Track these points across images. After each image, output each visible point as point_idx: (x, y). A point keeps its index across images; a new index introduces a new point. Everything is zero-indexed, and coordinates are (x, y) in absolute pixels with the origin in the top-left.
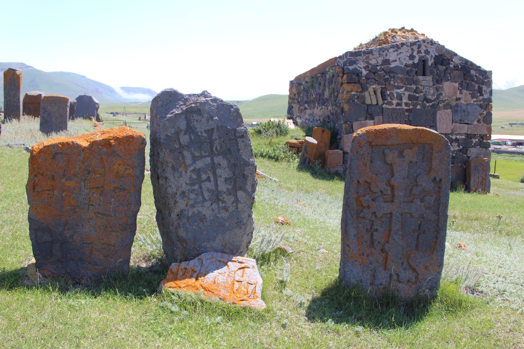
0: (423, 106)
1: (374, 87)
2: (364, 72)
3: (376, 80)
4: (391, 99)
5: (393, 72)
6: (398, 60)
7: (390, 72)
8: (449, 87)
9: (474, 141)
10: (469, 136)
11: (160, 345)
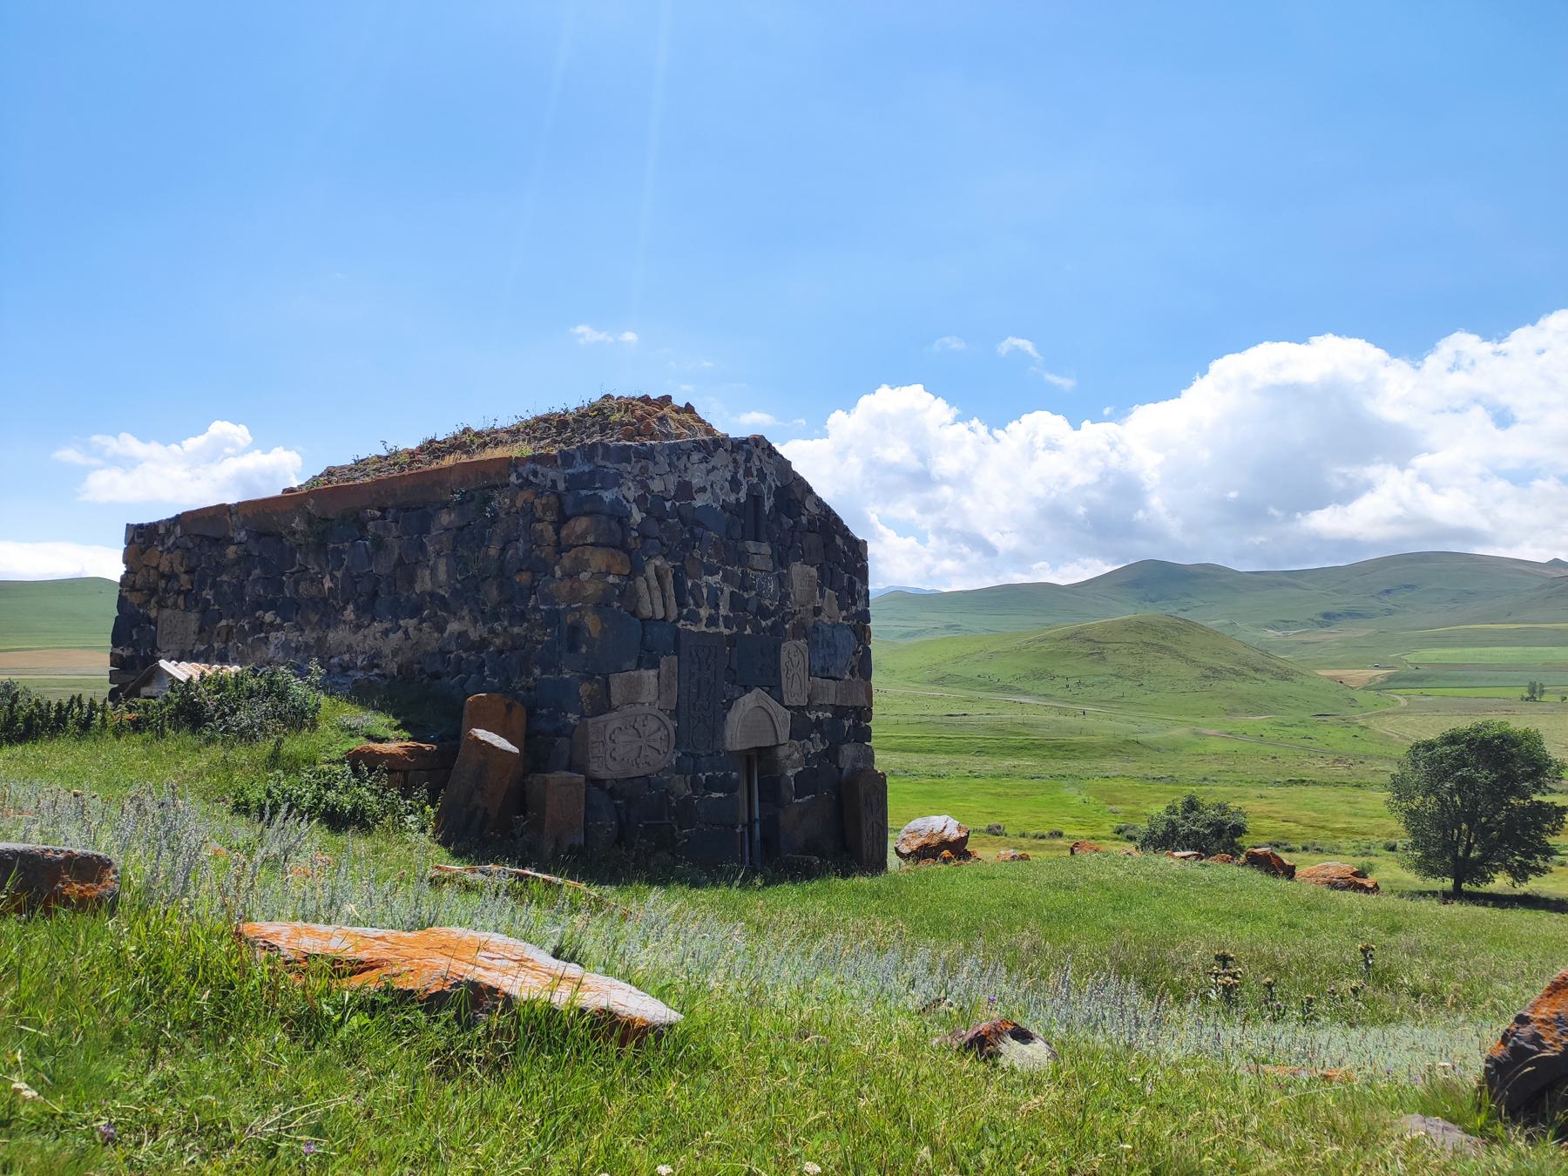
0: (757, 628)
2: (637, 516)
3: (663, 544)
5: (699, 524)
7: (693, 522)
10: (839, 712)
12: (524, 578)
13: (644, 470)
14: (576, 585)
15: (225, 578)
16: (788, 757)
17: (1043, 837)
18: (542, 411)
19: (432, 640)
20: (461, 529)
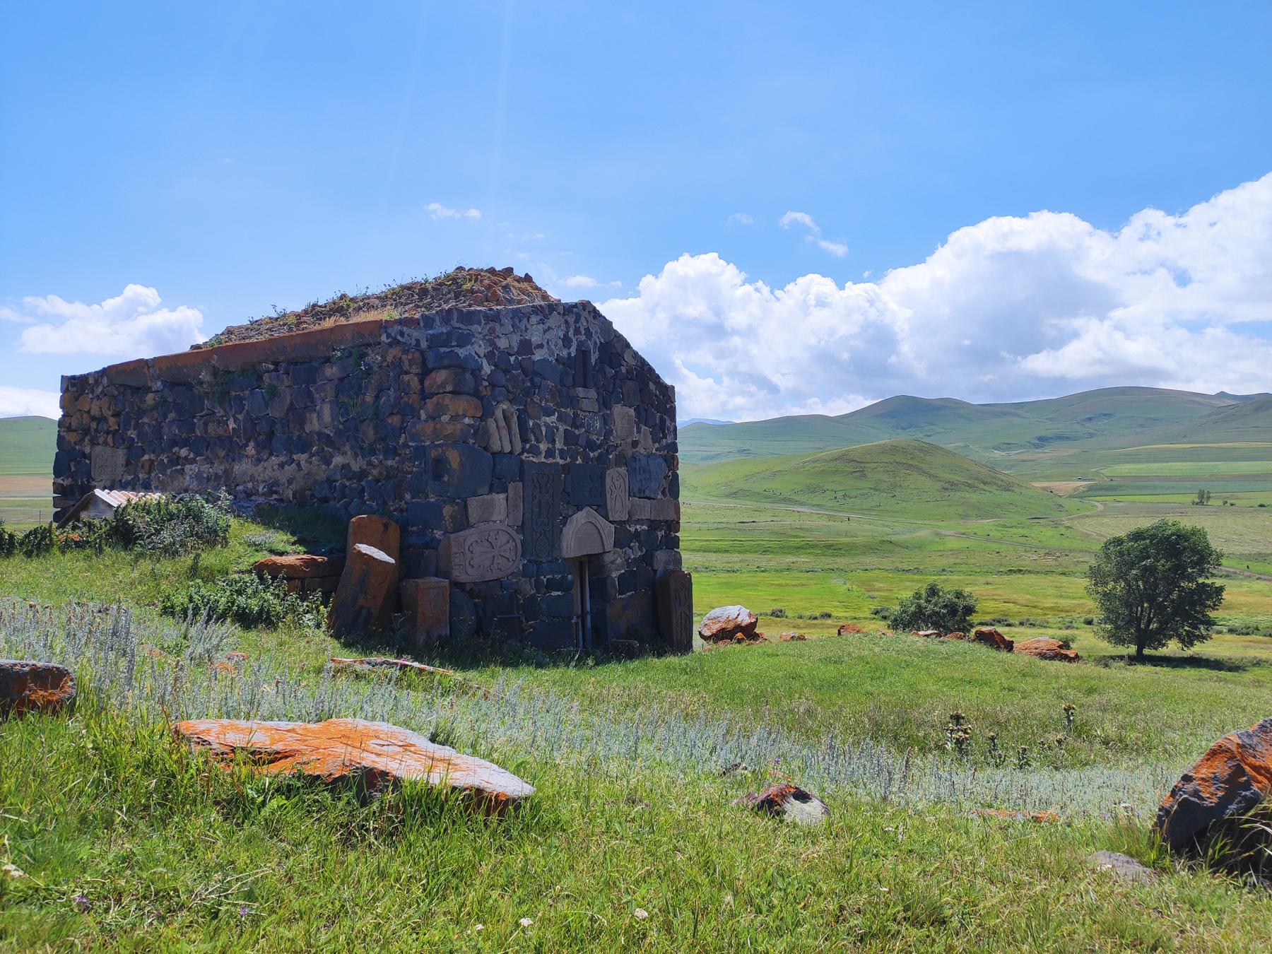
0: (586, 458)
2: (487, 369)
5: (538, 374)
7: (533, 372)
10: (654, 525)
12: (395, 420)
13: (492, 331)
14: (438, 426)
15: (146, 420)
16: (613, 562)
17: (816, 618)
18: (407, 281)
19: (321, 472)
20: (341, 380)
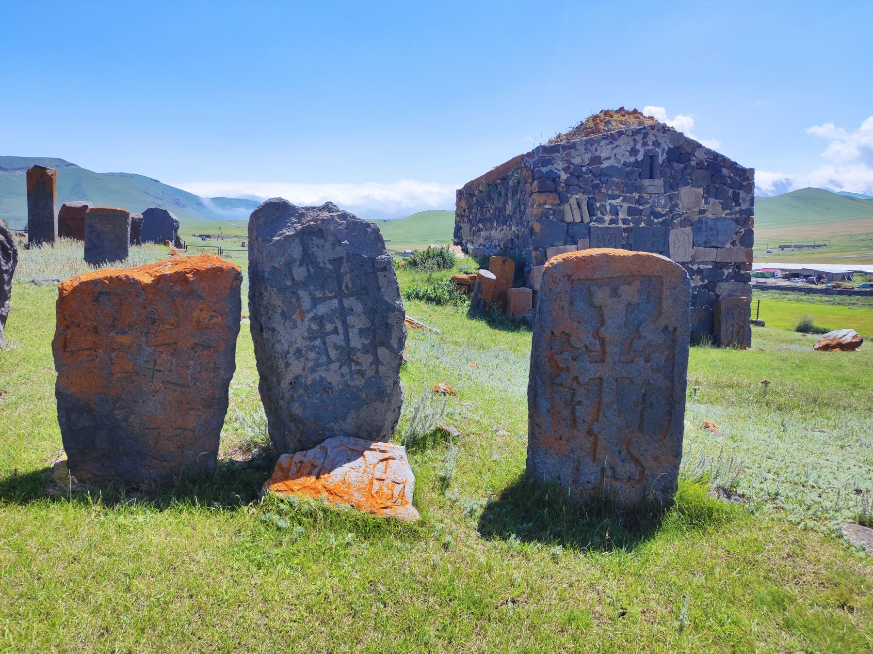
0: (650, 223)
1: (577, 196)
4: (602, 213)
6: (613, 157)
7: (602, 175)
8: (689, 197)
9: (726, 272)
10: (719, 266)
11: (259, 582)
